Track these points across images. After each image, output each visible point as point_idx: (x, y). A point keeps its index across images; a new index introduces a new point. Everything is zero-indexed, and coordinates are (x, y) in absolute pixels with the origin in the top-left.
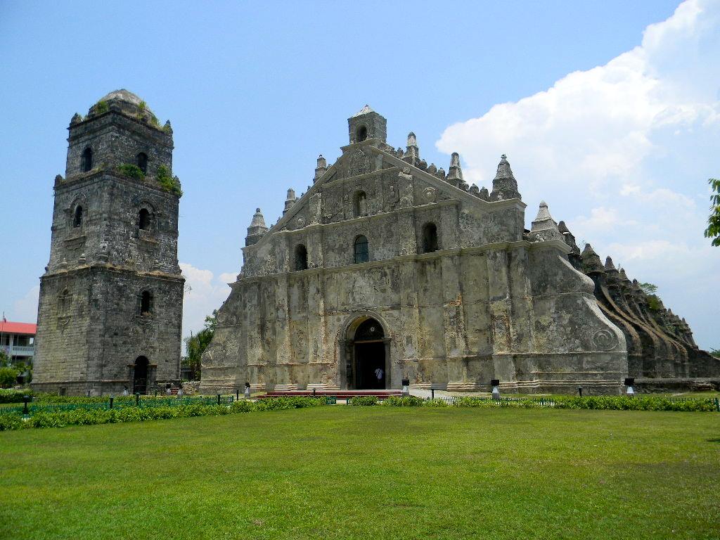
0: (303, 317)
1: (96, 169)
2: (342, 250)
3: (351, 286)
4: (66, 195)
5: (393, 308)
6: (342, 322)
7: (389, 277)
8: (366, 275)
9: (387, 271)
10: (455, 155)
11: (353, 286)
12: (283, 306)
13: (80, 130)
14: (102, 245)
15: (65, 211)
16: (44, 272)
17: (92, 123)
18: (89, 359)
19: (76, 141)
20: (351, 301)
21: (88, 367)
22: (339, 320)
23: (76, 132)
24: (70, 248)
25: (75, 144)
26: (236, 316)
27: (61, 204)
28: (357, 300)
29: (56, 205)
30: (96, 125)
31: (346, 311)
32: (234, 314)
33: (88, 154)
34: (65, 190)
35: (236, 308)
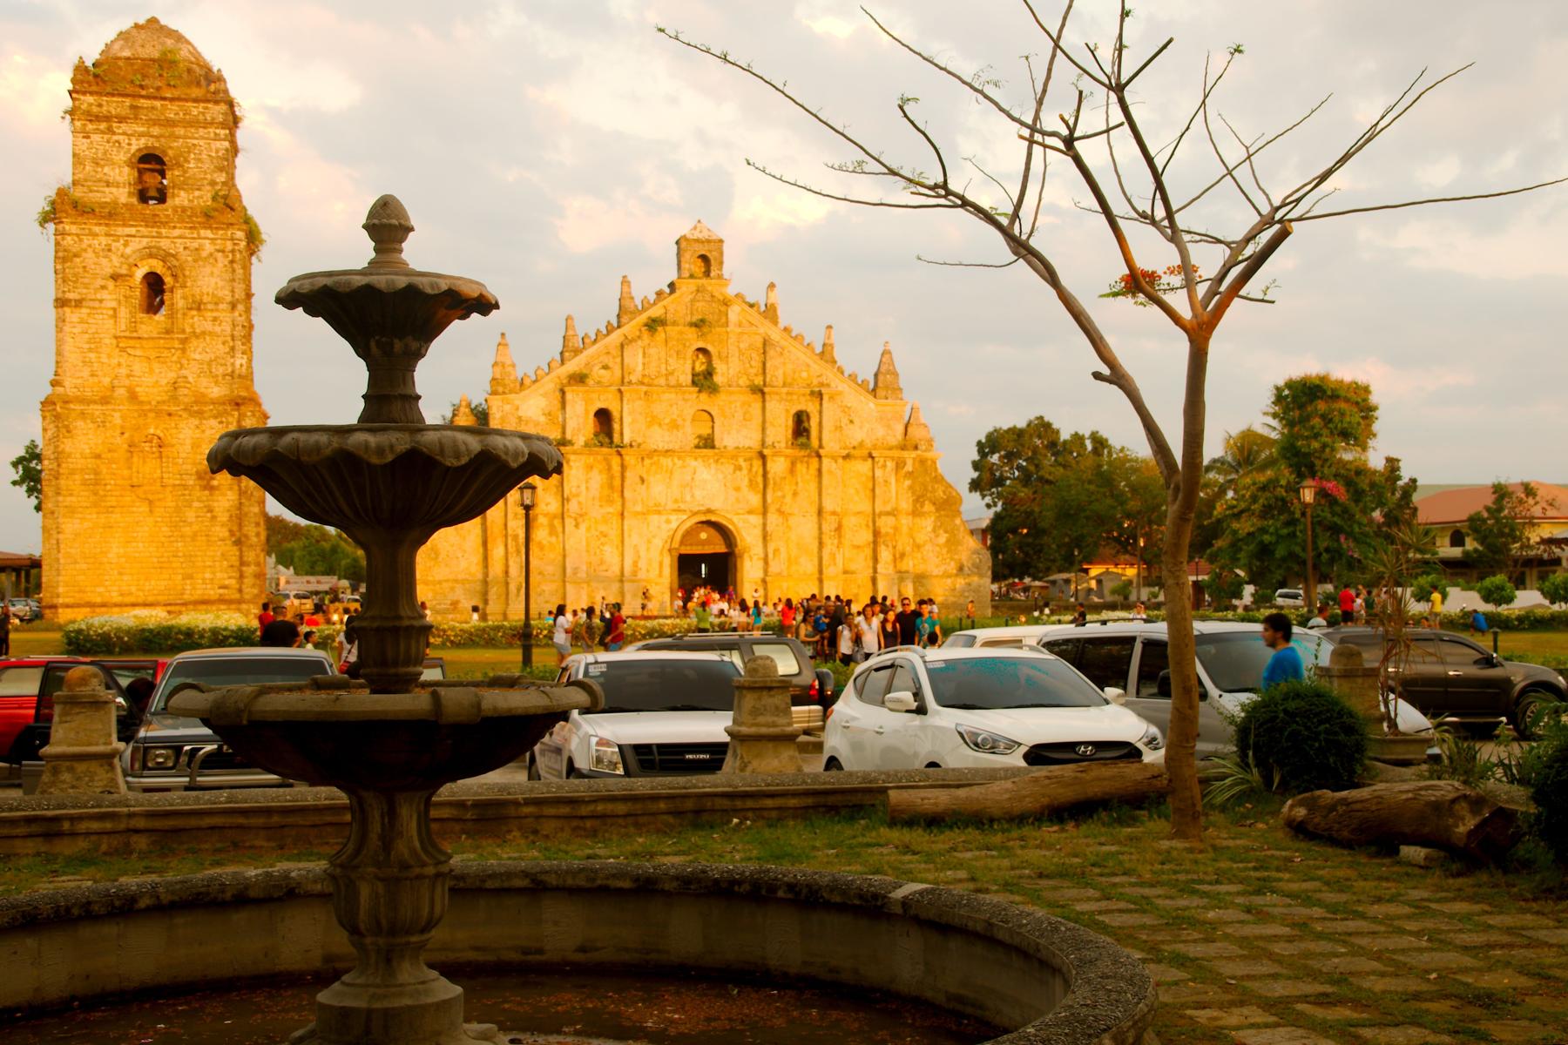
1: (179, 199)
2: (674, 426)
4: (104, 240)
5: (750, 512)
6: (674, 525)
7: (745, 472)
10: (829, 327)
13: (114, 106)
14: (238, 362)
15: (115, 277)
16: (48, 390)
17: (158, 104)
18: (242, 563)
19: (103, 126)
20: (688, 498)
21: (242, 576)
22: (668, 522)
23: (100, 105)
24: (138, 353)
25: (103, 132)
27: (90, 255)
29: (63, 257)
30: (172, 111)
31: (678, 511)
33: (151, 162)
34: (97, 229)
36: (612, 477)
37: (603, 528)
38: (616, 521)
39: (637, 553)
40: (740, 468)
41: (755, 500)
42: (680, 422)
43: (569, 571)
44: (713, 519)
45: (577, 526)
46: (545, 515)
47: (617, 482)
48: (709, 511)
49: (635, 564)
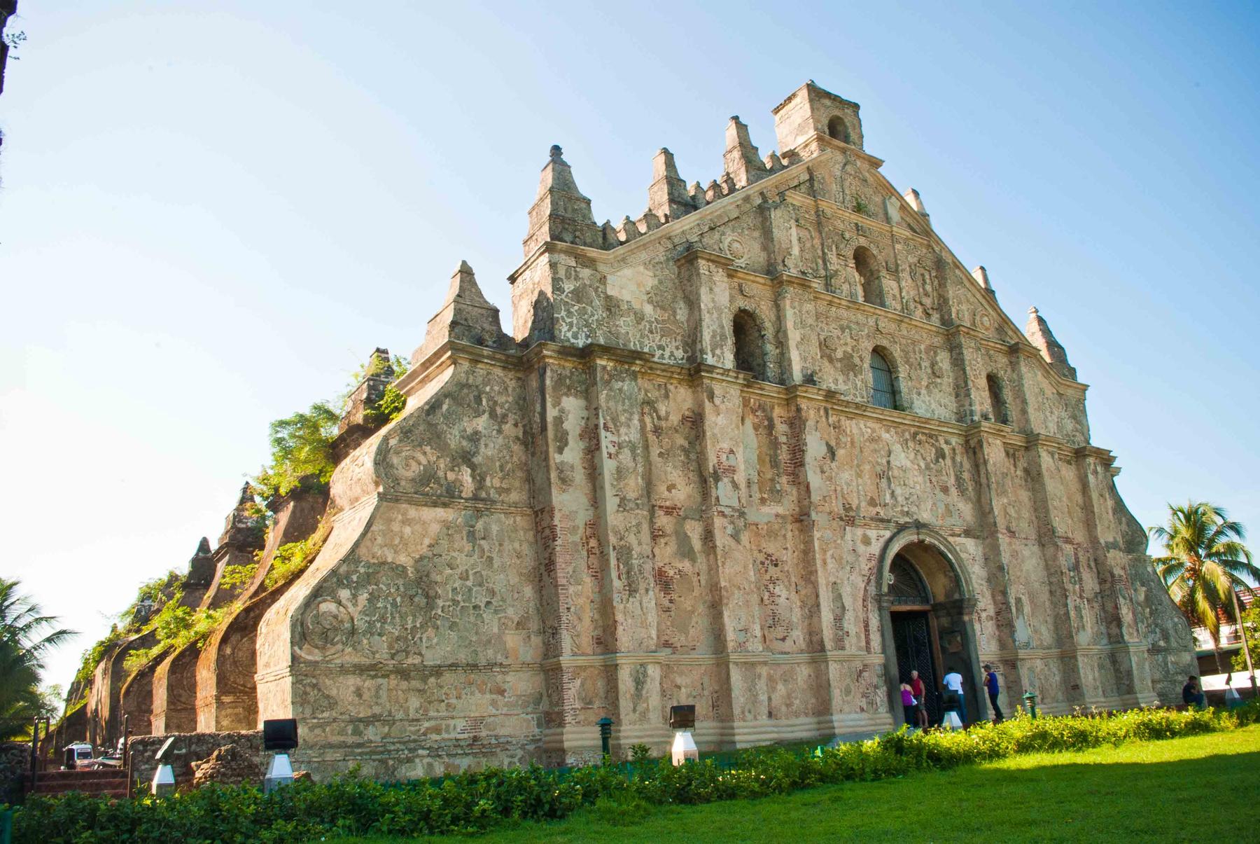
0: (777, 516)
3: (884, 461)
6: (876, 548)
7: (948, 461)
8: (911, 444)
9: (946, 448)
11: (888, 462)
12: (732, 470)
22: (866, 541)
26: (473, 467)
28: (900, 499)
31: (882, 521)
32: (466, 458)
35: (475, 438)
36: (775, 444)
37: (771, 547)
38: (790, 531)
39: (839, 597)
40: (944, 458)
41: (966, 510)
42: (857, 361)
43: (731, 636)
44: (928, 540)
45: (736, 537)
46: (669, 511)
47: (784, 455)
48: (919, 526)
49: (839, 619)
